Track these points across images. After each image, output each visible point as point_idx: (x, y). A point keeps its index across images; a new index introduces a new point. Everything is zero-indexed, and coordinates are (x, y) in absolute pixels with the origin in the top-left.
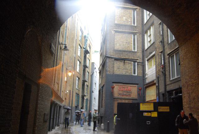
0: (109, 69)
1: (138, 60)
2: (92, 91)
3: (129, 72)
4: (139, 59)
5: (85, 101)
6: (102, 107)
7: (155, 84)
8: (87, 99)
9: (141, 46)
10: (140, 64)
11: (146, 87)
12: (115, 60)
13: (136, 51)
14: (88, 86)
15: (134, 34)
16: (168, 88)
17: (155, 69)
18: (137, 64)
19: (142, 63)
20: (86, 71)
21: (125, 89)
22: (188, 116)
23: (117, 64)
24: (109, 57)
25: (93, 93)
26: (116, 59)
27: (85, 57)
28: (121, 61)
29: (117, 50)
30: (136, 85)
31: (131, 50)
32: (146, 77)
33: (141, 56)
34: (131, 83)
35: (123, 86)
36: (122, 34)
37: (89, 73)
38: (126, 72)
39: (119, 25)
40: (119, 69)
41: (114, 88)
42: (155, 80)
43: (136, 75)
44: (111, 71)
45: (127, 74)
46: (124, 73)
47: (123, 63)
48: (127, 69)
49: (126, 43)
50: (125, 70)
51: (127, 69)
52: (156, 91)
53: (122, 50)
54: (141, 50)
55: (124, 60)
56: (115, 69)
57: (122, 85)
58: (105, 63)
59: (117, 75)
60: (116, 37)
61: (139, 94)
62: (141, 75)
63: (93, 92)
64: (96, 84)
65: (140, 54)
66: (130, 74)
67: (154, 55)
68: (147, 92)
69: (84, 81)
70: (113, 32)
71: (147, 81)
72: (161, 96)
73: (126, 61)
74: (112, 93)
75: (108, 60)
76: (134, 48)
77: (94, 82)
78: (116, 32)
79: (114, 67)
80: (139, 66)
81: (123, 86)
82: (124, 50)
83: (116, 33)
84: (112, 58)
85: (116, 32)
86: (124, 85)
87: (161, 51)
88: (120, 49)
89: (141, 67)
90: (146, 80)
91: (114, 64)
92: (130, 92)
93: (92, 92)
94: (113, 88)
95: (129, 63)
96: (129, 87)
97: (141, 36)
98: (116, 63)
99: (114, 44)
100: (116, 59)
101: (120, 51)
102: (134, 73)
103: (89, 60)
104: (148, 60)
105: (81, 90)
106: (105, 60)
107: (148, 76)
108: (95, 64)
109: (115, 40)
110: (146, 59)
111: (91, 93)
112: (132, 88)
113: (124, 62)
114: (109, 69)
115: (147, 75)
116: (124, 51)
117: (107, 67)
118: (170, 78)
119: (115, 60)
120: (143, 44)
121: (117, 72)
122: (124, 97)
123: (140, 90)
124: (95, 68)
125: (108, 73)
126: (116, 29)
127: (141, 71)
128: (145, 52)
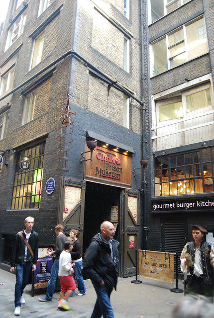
3: (118, 117)
22: (65, 216)
23: (96, 88)
24: (79, 59)
28: (103, 84)
29: (95, 51)
32: (152, 138)
33: (138, 89)
45: (113, 120)
46: (107, 116)
47: (106, 89)
51: (113, 108)
62: (137, 130)
75: (75, 65)
79: (87, 90)
82: (109, 58)
95: (116, 95)
104: (156, 101)
110: (154, 98)
114: (76, 91)
116: (110, 61)
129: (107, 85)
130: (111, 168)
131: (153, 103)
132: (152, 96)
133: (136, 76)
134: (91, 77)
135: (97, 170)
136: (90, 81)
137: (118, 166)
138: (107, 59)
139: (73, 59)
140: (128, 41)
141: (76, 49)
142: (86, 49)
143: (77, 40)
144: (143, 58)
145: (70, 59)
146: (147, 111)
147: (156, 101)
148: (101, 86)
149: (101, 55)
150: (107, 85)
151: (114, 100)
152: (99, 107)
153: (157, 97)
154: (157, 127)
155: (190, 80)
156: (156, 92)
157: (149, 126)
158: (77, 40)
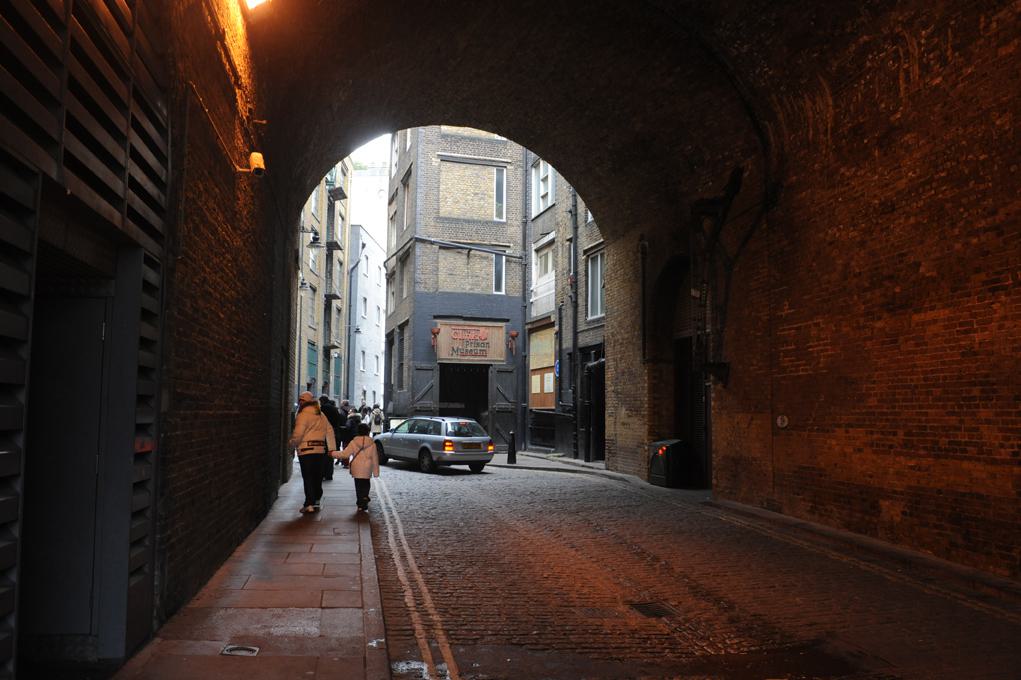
0: (423, 277)
1: (509, 247)
2: (353, 330)
3: (484, 284)
4: (512, 245)
5: (332, 362)
6: (401, 386)
7: (552, 325)
8: (339, 357)
9: (519, 204)
11: (532, 331)
12: (441, 248)
14: (339, 311)
15: (500, 167)
16: (585, 340)
17: (554, 282)
18: (507, 261)
19: (521, 258)
20: (335, 261)
21: (472, 335)
23: (447, 260)
25: (357, 335)
26: (444, 247)
27: (331, 208)
29: (446, 219)
31: (489, 219)
33: (519, 237)
34: (487, 317)
36: (464, 166)
37: (341, 264)
38: (472, 285)
39: (452, 136)
40: (453, 276)
41: (438, 333)
43: (503, 293)
44: (430, 282)
45: (477, 291)
46: (467, 288)
49: (476, 194)
53: (462, 217)
54: (519, 217)
56: (442, 276)
57: (462, 322)
59: (447, 293)
60: (443, 176)
61: (510, 350)
62: (518, 294)
63: (358, 331)
64: (365, 300)
65: (515, 231)
66: (484, 292)
67: (552, 242)
68: (531, 343)
69: (330, 298)
70: (436, 162)
72: (566, 357)
74: (432, 349)
75: (419, 249)
77: (360, 295)
78: (444, 159)
82: (468, 216)
83: (444, 163)
84: (432, 243)
85: (444, 159)
86: (468, 323)
87: (568, 237)
88: (456, 213)
89: (518, 269)
90: (530, 311)
91: (437, 261)
92: (484, 343)
93: (352, 331)
94: (436, 334)
96: (480, 329)
97: (520, 171)
98: (445, 259)
99: (438, 201)
100: (444, 247)
101: (457, 220)
102: (498, 287)
103: (343, 219)
104: (537, 251)
105: (321, 328)
106: (408, 245)
108: (361, 231)
109: (442, 187)
110: (534, 247)
111: (349, 336)
114: (423, 277)
115: (536, 294)
116: (468, 221)
119: (441, 248)
120: (526, 200)
121: (447, 285)
122: (466, 358)
123: (513, 337)
124: (364, 246)
125: (420, 288)
126: (445, 150)
127: (519, 283)
128: (530, 224)
138: (465, 220)
142: (432, 224)
145: (412, 247)
147: (537, 251)
148: (458, 256)
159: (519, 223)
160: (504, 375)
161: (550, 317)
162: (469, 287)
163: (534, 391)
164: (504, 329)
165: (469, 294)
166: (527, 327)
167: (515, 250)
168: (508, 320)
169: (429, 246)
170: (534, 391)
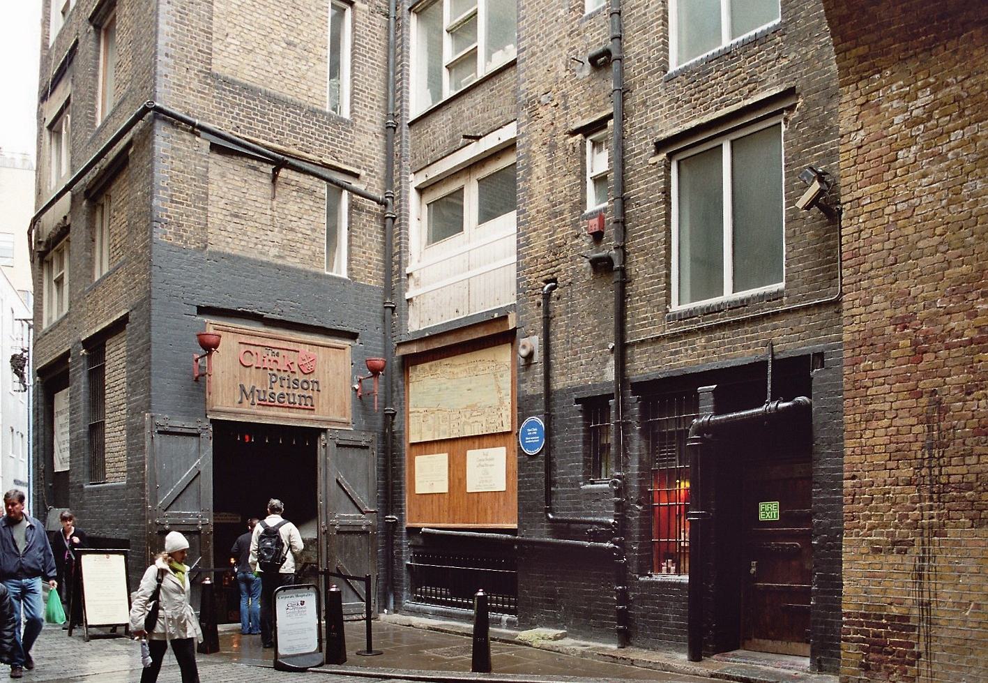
0: (172, 209)
1: (357, 176)
3: (305, 251)
4: (363, 173)
7: (509, 337)
9: (375, 85)
10: (367, 203)
11: (409, 362)
12: (214, 147)
13: (346, 114)
16: (644, 366)
18: (353, 206)
24: (175, 121)
26: (225, 148)
28: (255, 168)
29: (226, 81)
30: (346, 343)
32: (407, 296)
33: (377, 159)
34: (315, 323)
35: (271, 343)
38: (283, 247)
41: (216, 346)
42: (513, 307)
44: (190, 223)
45: (291, 262)
46: (271, 254)
47: (266, 181)
48: (292, 230)
50: (276, 235)
51: (292, 230)
52: (517, 382)
55: (279, 162)
56: (216, 215)
57: (262, 330)
58: (133, 168)
61: (362, 400)
62: (373, 279)
71: (416, 323)
72: (572, 414)
73: (284, 173)
74: (199, 382)
75: (163, 139)
76: (336, 93)
80: (365, 217)
81: (271, 343)
82: (275, 88)
84: (196, 129)
89: (372, 233)
91: (205, 178)
92: (306, 381)
94: (209, 347)
96: (301, 347)
98: (223, 176)
100: (225, 148)
104: (421, 191)
107: (419, 291)
112: (320, 354)
113: (274, 178)
114: (172, 209)
115: (417, 283)
116: (276, 100)
117: (161, 193)
118: (668, 302)
121: (228, 241)
123: (375, 372)
129: (269, 169)
130: (285, 383)
131: (413, 196)
132: (412, 177)
133: (373, 121)
134: (218, 157)
135: (243, 389)
136: (214, 174)
137: (306, 377)
138: (267, 95)
139: (158, 123)
140: (349, 11)
141: (165, 100)
142: (195, 84)
143: (167, 65)
144: (391, 60)
145: (147, 134)
146: (397, 222)
147: (421, 191)
148: (251, 177)
149: (245, 88)
150: (269, 169)
151: (292, 207)
152: (244, 234)
153: (420, 180)
154: (422, 264)
155: (480, 137)
156: (419, 167)
157: (399, 263)
158: (167, 65)
159: (377, 128)
160: (351, 454)
161: (504, 318)
162: (274, 251)
163: (421, 488)
164: (348, 350)
165: (279, 267)
166: (403, 351)
167: (371, 184)
168: (353, 336)
169: (187, 136)
170: (421, 488)
